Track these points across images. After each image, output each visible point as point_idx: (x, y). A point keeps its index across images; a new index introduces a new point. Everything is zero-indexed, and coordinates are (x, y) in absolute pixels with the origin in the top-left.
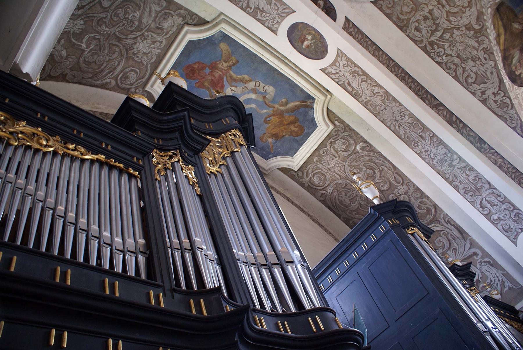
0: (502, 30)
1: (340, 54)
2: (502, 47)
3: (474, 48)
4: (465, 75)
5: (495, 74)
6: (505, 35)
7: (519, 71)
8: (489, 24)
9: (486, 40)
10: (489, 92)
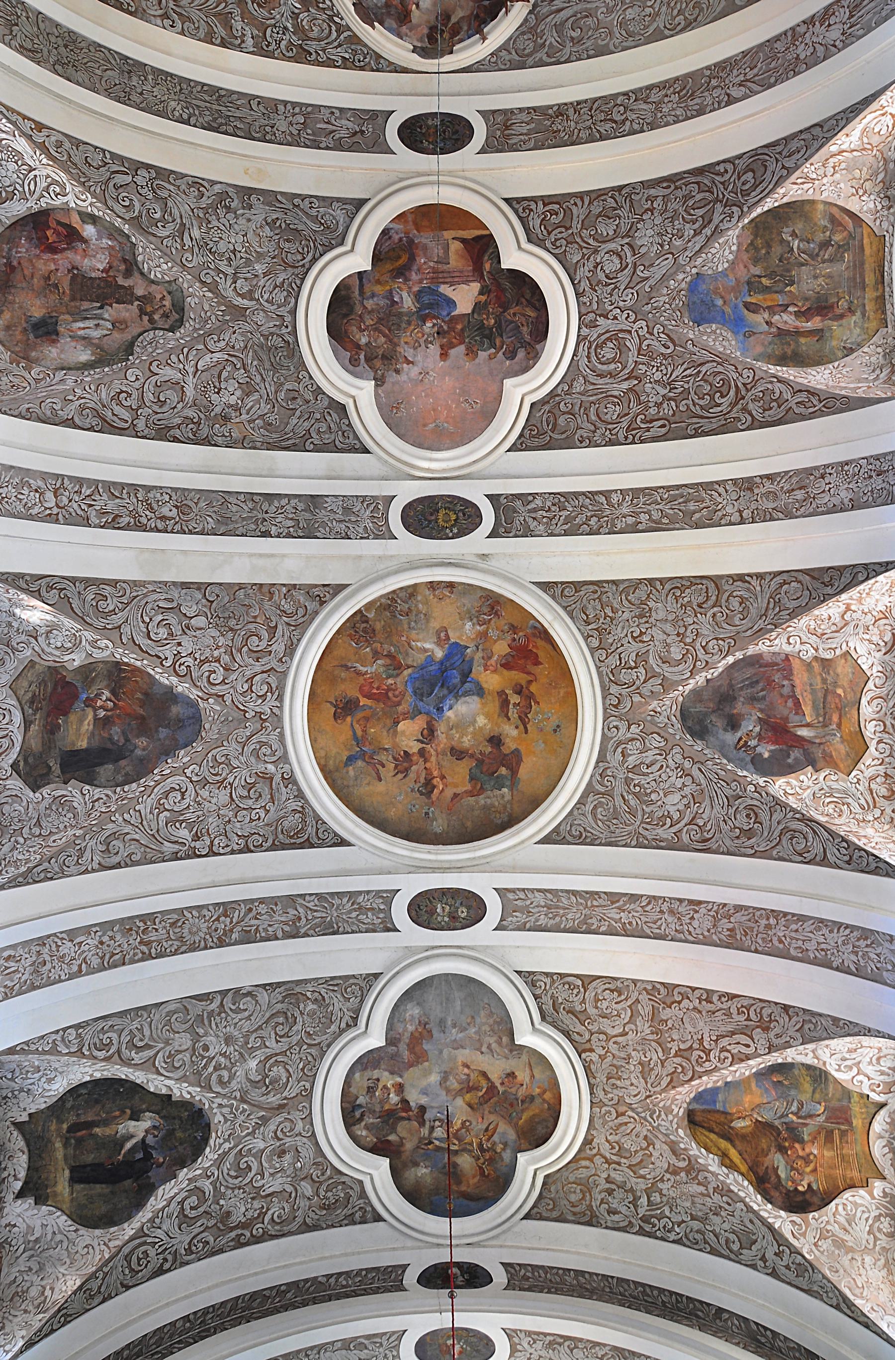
0: (724, 1144)
1: (510, 1334)
2: (744, 1168)
3: (702, 1194)
4: (723, 1242)
5: (756, 1221)
6: (734, 1146)
7: (805, 1183)
8: (694, 1150)
9: (710, 1177)
10: (770, 1255)
